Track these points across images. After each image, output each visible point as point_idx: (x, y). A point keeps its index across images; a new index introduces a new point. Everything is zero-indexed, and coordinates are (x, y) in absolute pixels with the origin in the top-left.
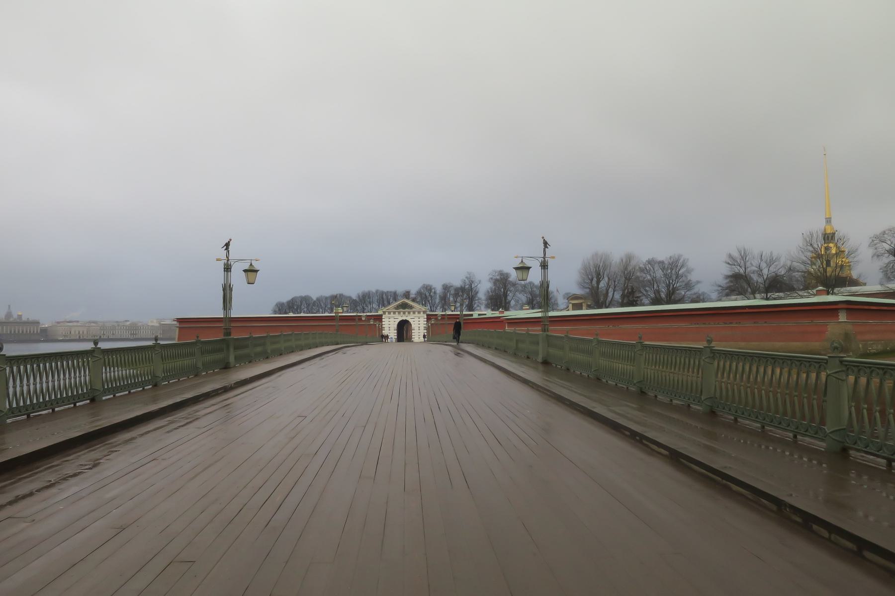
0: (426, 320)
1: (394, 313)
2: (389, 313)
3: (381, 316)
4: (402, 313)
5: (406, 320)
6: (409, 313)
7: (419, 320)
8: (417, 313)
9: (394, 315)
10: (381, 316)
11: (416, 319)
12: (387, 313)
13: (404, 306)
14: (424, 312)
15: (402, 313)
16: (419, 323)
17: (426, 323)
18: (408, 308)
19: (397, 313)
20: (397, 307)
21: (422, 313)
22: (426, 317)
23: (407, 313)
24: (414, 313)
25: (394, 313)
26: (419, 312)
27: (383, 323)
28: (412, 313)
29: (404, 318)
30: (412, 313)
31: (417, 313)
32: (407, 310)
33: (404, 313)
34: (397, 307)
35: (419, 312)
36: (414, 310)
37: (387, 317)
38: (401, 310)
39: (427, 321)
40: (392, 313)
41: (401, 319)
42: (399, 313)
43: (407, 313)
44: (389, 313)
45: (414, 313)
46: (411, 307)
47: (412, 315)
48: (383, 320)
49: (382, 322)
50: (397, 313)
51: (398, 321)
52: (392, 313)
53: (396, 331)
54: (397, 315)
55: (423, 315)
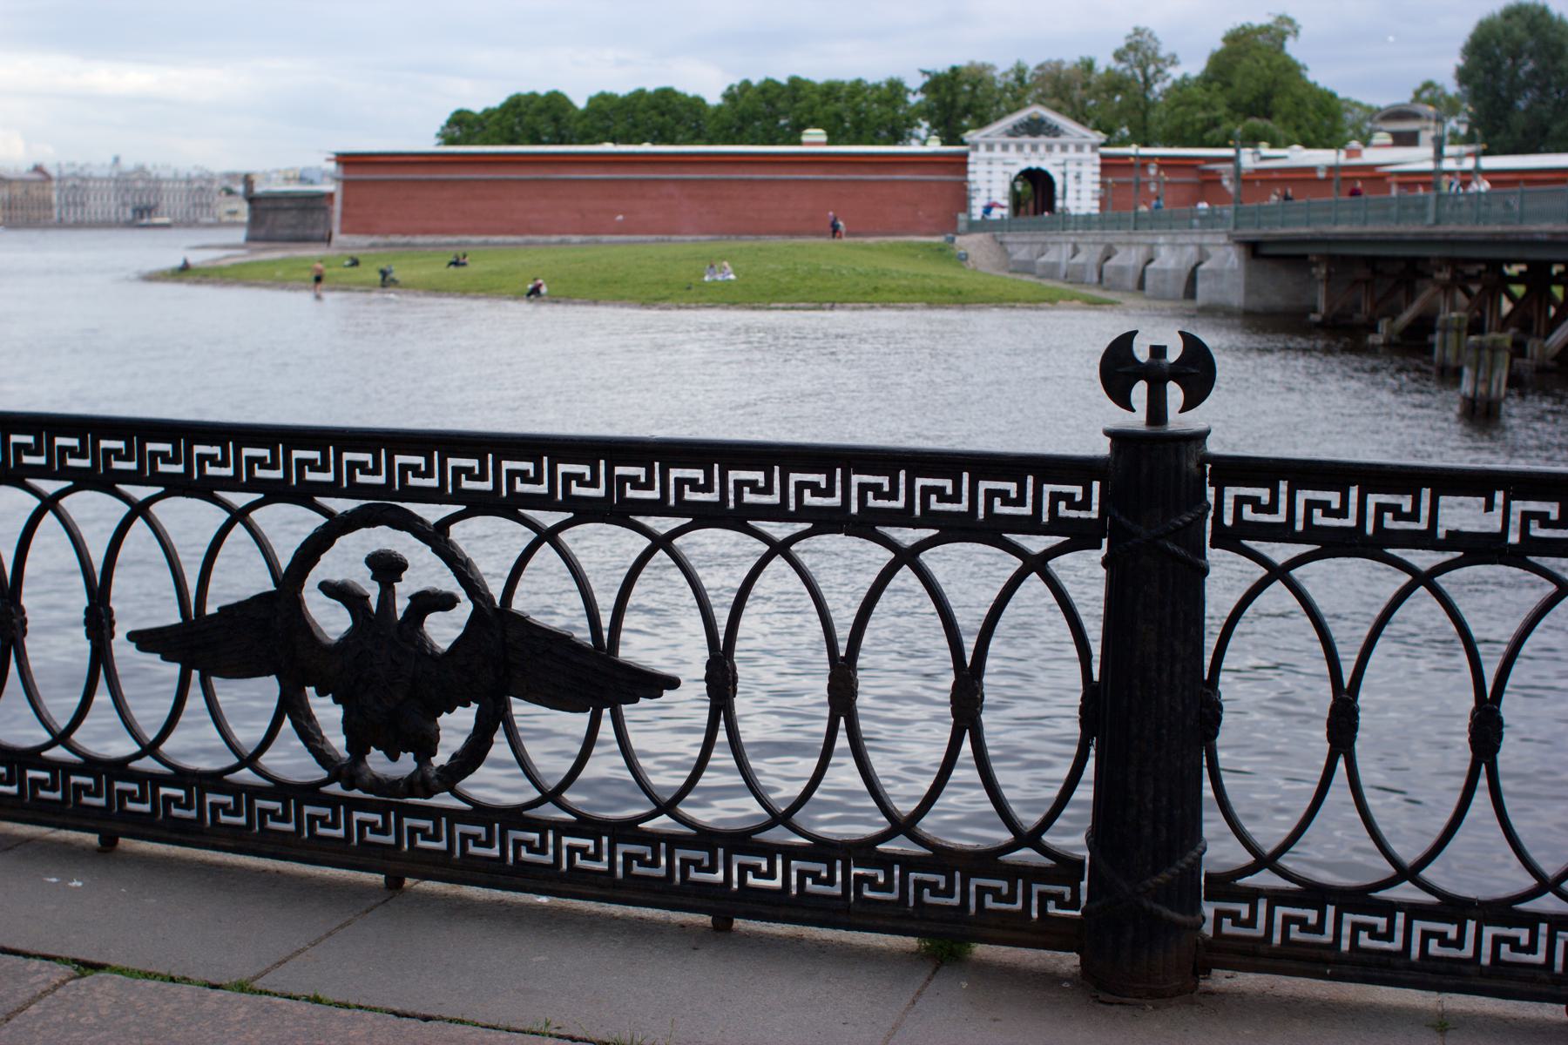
0: (1098, 169)
1: (1005, 147)
2: (990, 147)
3: (965, 155)
4: (1027, 149)
6: (1049, 148)
8: (1072, 149)
9: (1004, 155)
12: (982, 148)
14: (1094, 148)
15: (1027, 149)
17: (1098, 178)
18: (1047, 135)
19: (1012, 148)
20: (1015, 131)
21: (1087, 149)
22: (1098, 161)
23: (1042, 149)
24: (1064, 148)
25: (1005, 147)
26: (1079, 148)
28: (1057, 149)
29: (1034, 164)
30: (1057, 149)
31: (1072, 149)
32: (1042, 139)
33: (1034, 148)
34: (1015, 131)
35: (1079, 148)
36: (1063, 139)
37: (983, 159)
38: (1026, 139)
39: (1103, 174)
40: (998, 148)
42: (1020, 148)
43: (1042, 149)
44: (990, 147)
45: (1064, 148)
46: (1055, 131)
47: (1058, 156)
48: (971, 168)
49: (966, 172)
50: (1012, 148)
52: (998, 148)
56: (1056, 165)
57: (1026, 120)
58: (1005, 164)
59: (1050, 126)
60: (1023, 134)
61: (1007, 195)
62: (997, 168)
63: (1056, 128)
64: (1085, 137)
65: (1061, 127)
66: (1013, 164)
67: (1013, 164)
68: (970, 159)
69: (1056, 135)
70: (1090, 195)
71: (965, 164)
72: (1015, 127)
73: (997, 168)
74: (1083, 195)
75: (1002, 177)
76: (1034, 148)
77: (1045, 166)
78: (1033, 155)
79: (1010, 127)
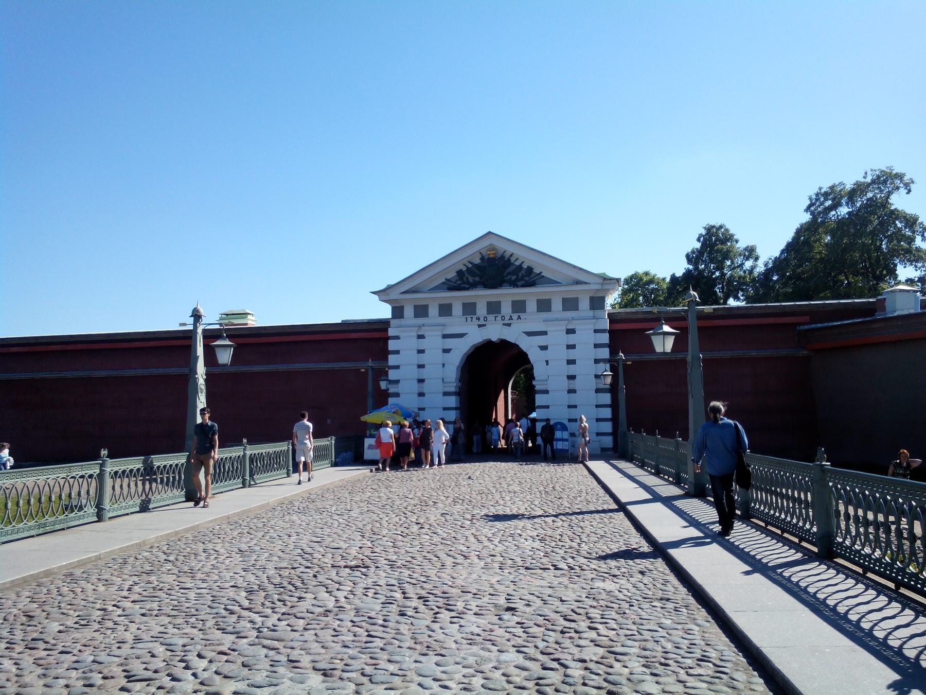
0: (605, 338)
2: (421, 311)
6: (519, 307)
7: (572, 339)
17: (605, 353)
18: (514, 284)
21: (584, 304)
25: (446, 310)
26: (570, 304)
27: (392, 360)
29: (495, 332)
32: (506, 295)
38: (482, 296)
39: (613, 347)
41: (475, 336)
42: (469, 309)
44: (421, 311)
45: (544, 306)
47: (533, 320)
48: (392, 345)
49: (384, 353)
51: (461, 348)
53: (452, 401)
54: (456, 322)
55: (591, 313)
56: (530, 334)
57: (477, 261)
58: (445, 336)
59: (520, 267)
60: (473, 286)
63: (530, 269)
64: (578, 282)
65: (537, 271)
66: (461, 336)
67: (461, 336)
68: (391, 332)
69: (532, 284)
70: (593, 384)
71: (388, 338)
72: (460, 273)
75: (440, 357)
76: (494, 308)
77: (514, 334)
78: (491, 317)
79: (452, 275)
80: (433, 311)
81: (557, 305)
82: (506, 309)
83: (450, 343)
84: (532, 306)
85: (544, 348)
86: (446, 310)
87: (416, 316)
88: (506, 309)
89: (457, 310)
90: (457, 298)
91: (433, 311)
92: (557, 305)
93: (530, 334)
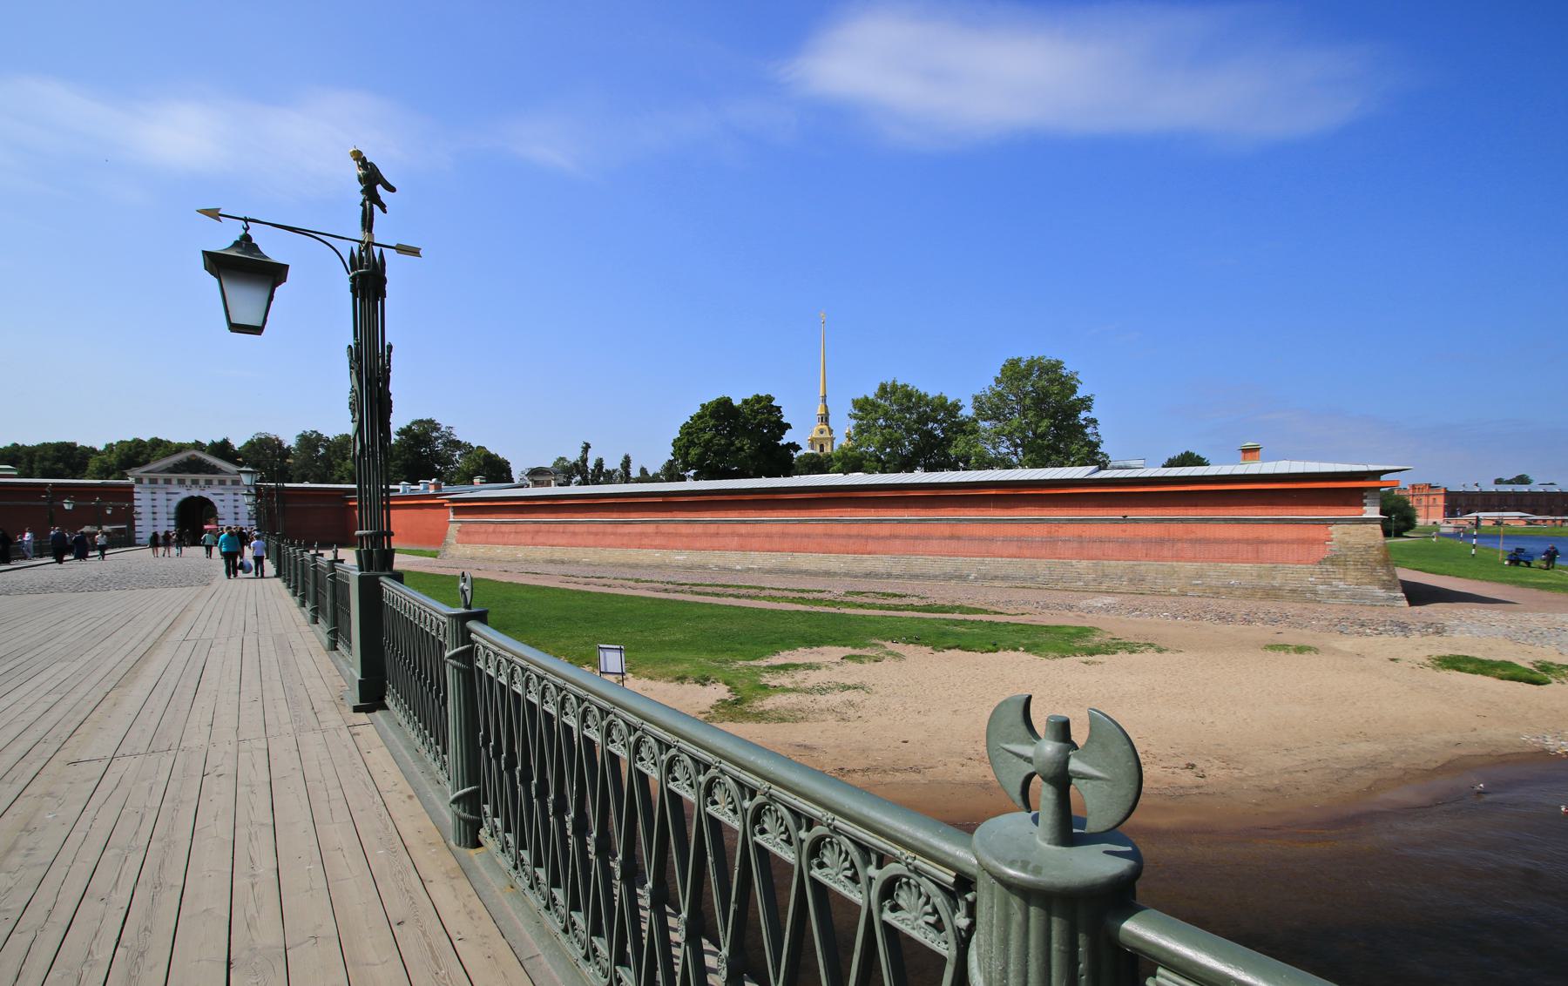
2: (153, 481)
5: (200, 498)
6: (209, 482)
9: (166, 486)
10: (132, 487)
11: (229, 496)
12: (146, 481)
13: (195, 466)
16: (237, 504)
18: (207, 473)
29: (195, 492)
32: (202, 477)
34: (176, 469)
38: (189, 477)
41: (184, 493)
42: (181, 482)
45: (222, 482)
46: (215, 470)
48: (136, 496)
49: (132, 500)
51: (177, 499)
54: (174, 488)
56: (214, 494)
57: (185, 460)
58: (167, 493)
61: (173, 516)
62: (161, 497)
68: (135, 490)
72: (175, 465)
73: (161, 497)
74: (239, 516)
76: (195, 482)
78: (193, 486)
79: (171, 466)
80: (161, 482)
81: (229, 483)
82: (202, 483)
83: (170, 496)
84: (215, 482)
85: (222, 501)
86: (168, 481)
87: (150, 483)
88: (202, 483)
89: (175, 482)
90: (175, 477)
91: (161, 482)
92: (229, 483)
93: (214, 494)
